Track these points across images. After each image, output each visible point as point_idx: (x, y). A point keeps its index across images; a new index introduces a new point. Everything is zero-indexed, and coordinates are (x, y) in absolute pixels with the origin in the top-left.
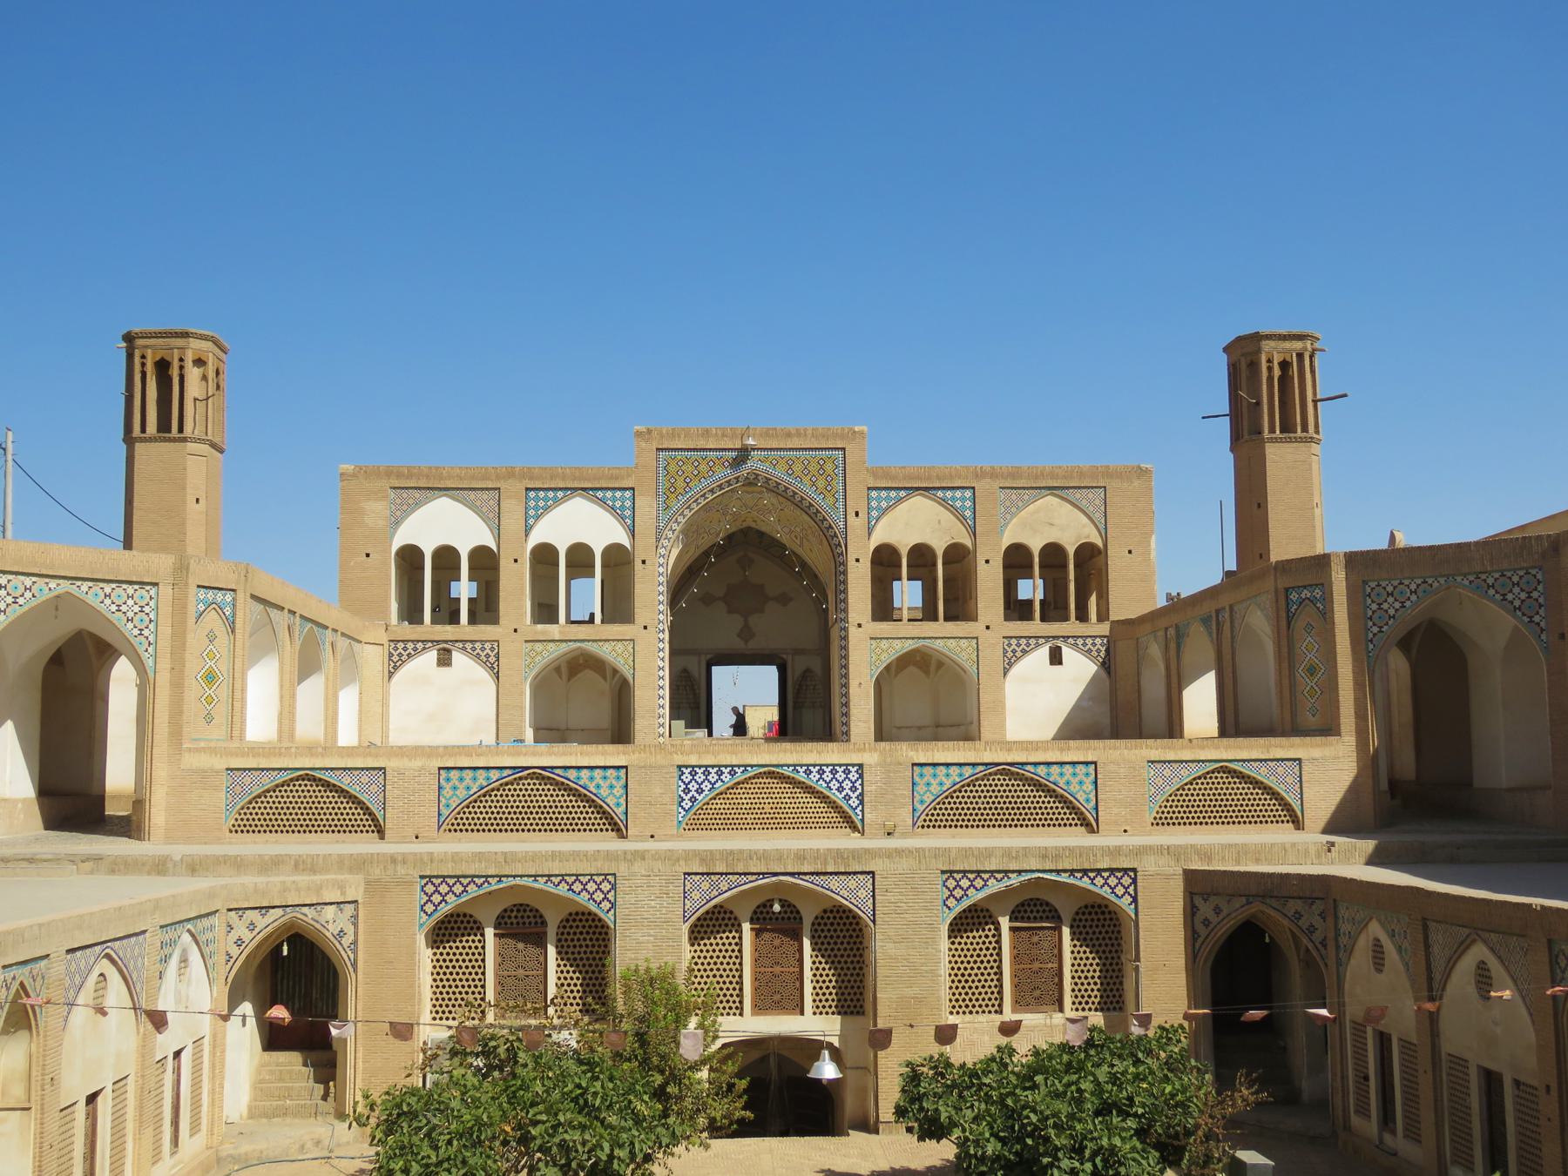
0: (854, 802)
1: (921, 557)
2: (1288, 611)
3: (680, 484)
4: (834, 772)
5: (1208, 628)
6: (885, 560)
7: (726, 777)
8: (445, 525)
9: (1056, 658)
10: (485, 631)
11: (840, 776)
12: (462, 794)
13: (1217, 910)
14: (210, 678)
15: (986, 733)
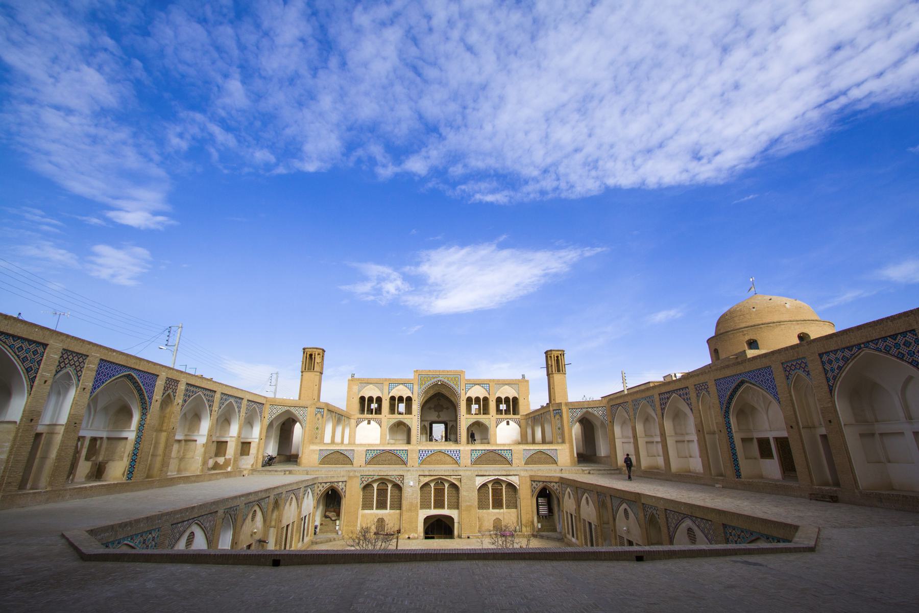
1: (477, 400)
6: (469, 400)
9: (508, 423)
10: (378, 416)
15: (492, 441)
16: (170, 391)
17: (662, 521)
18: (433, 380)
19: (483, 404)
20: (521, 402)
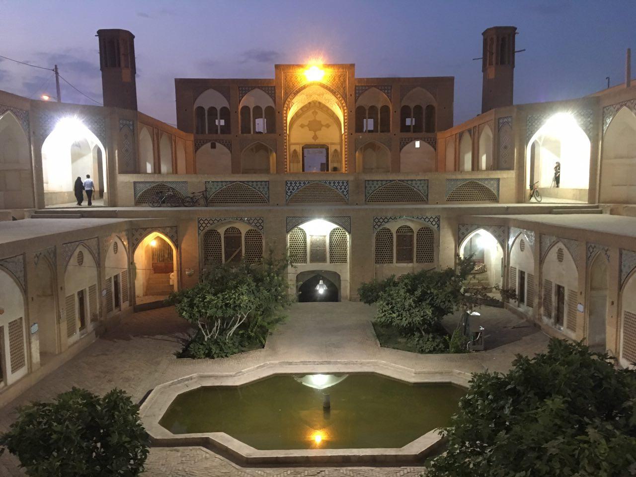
2: (499, 126)
4: (339, 183)
5: (470, 134)
7: (302, 185)
8: (211, 100)
11: (341, 184)
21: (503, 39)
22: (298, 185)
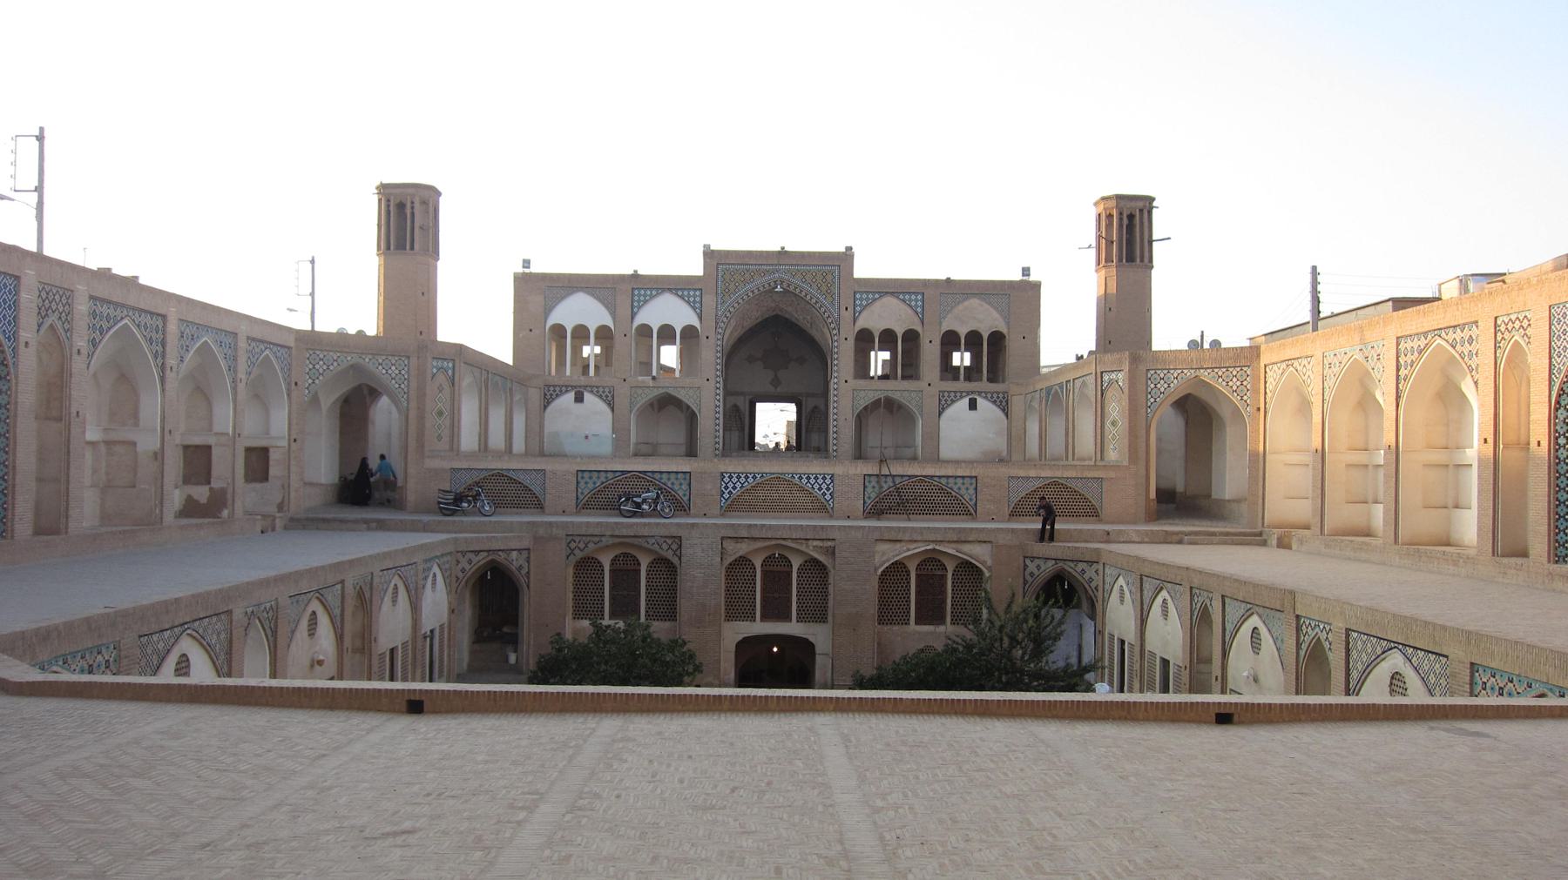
0: (828, 497)
3: (732, 286)
7: (750, 480)
9: (973, 405)
11: (820, 481)
12: (591, 486)
13: (1038, 567)
14: (440, 413)
16: (52, 319)
17: (1336, 658)
18: (759, 281)
19: (906, 347)
20: (1013, 346)
21: (1131, 217)
22: (743, 480)
